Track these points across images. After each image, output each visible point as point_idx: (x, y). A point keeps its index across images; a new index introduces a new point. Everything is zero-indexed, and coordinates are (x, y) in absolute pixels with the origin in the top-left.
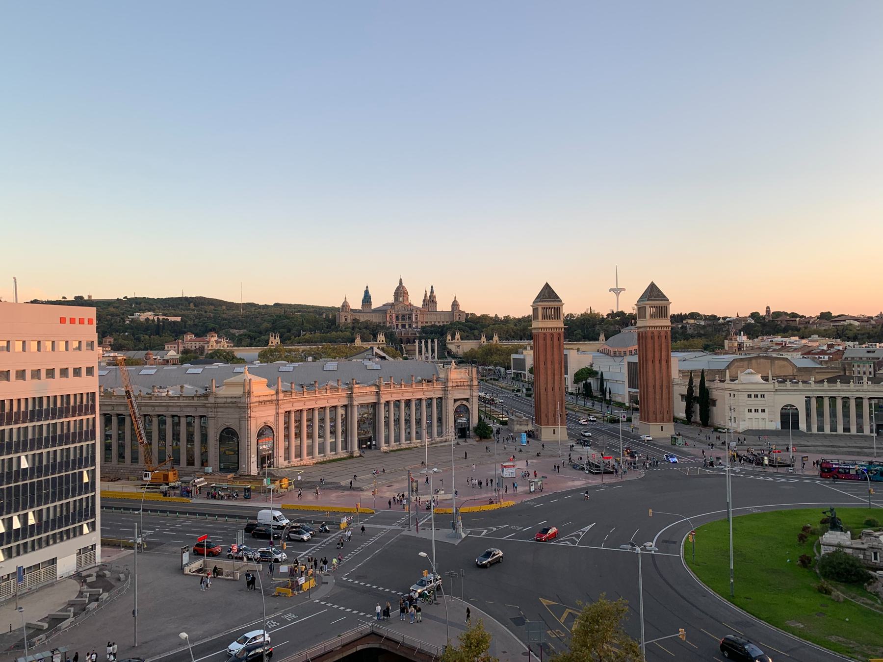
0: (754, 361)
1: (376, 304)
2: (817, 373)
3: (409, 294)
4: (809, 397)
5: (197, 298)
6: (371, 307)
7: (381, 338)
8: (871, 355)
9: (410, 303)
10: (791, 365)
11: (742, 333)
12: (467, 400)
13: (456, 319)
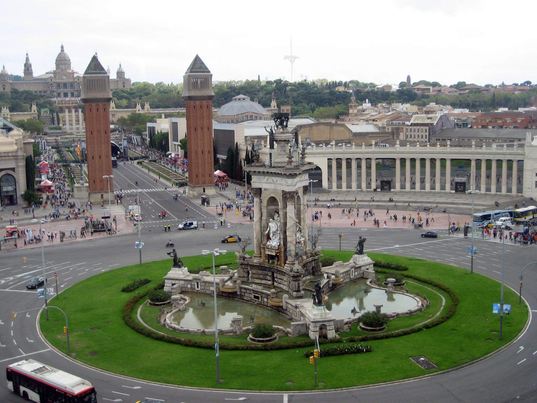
0: (314, 128)
1: (38, 72)
2: (370, 137)
3: (71, 61)
4: (331, 159)
6: (31, 73)
7: (34, 107)
8: (428, 121)
9: (73, 70)
10: (348, 131)
11: (367, 100)
12: (13, 169)
13: (121, 87)
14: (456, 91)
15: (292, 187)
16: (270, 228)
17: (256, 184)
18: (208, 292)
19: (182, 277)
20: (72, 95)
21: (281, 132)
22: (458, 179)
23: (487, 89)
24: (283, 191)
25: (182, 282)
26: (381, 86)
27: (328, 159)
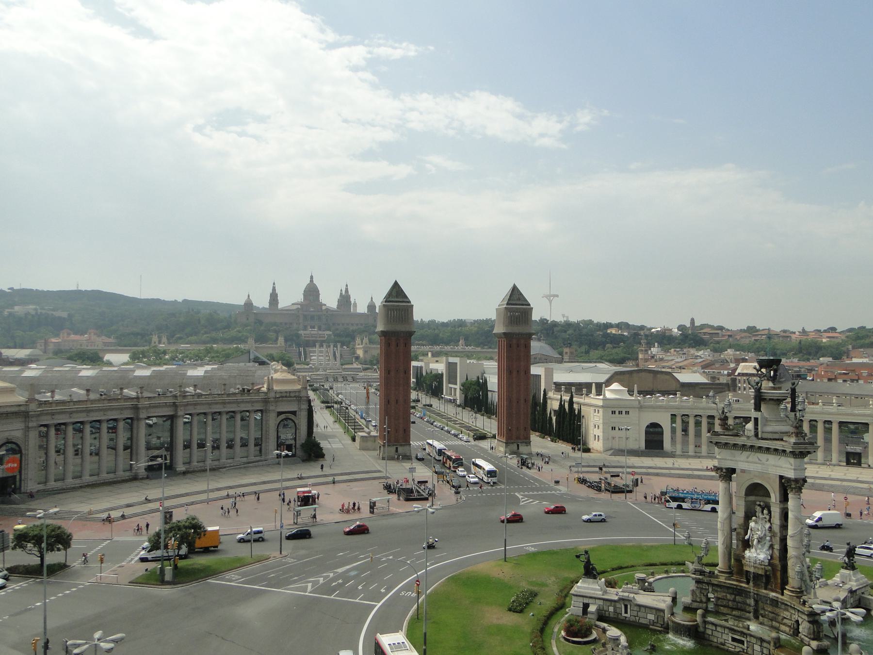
0: (635, 375)
1: (284, 302)
5: (93, 291)
7: (281, 340)
11: (656, 344)
14: (750, 337)
18: (642, 621)
19: (599, 594)
20: (320, 329)
21: (772, 387)
22: (851, 448)
23: (784, 334)
24: (781, 477)
25: (601, 602)
26: (659, 329)
27: (671, 415)
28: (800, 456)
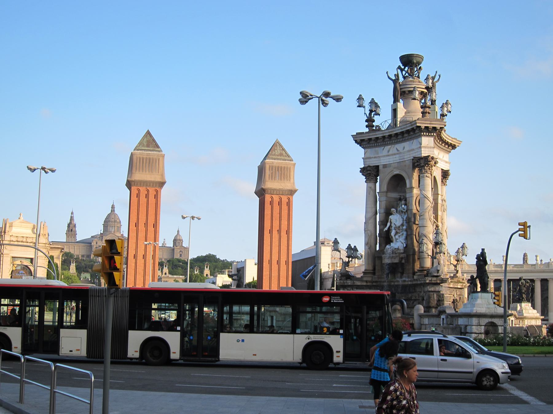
9: (122, 235)
13: (177, 256)
15: (429, 150)
16: (391, 223)
17: (371, 160)
28: (427, 134)
